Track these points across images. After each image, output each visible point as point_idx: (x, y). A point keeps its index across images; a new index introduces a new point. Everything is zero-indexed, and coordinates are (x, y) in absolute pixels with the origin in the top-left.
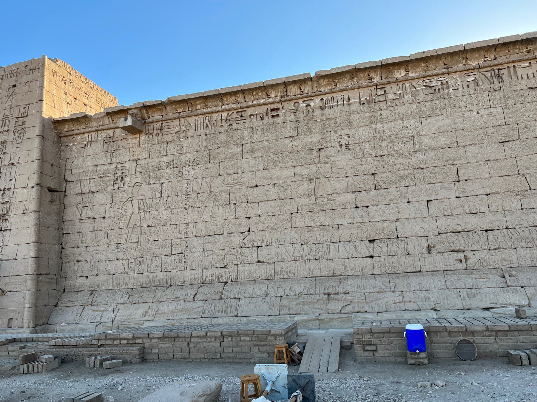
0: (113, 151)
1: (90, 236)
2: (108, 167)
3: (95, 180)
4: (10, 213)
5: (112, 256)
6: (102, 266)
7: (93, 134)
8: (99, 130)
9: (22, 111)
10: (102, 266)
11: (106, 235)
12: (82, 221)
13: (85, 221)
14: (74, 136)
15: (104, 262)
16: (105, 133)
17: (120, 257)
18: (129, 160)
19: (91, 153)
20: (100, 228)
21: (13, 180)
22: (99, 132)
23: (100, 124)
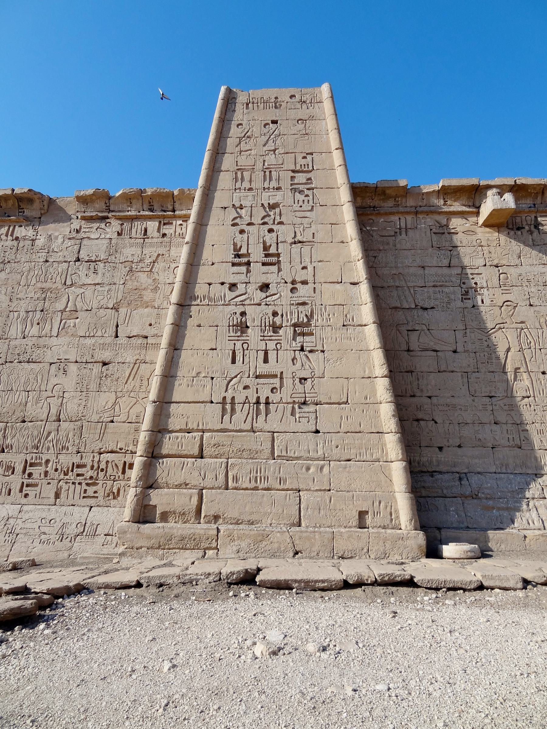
0: (451, 248)
1: (433, 379)
2: (446, 271)
3: (426, 290)
4: (313, 323)
5: (486, 417)
6: (467, 432)
7: (409, 218)
8: (422, 212)
9: (300, 161)
10: (467, 432)
11: (466, 380)
12: (411, 353)
13: (419, 353)
14: (370, 217)
15: (471, 425)
16: (431, 218)
17: (502, 418)
18: (485, 265)
19: (408, 246)
20: (450, 368)
21: (310, 268)
22: (421, 216)
23: (420, 204)
